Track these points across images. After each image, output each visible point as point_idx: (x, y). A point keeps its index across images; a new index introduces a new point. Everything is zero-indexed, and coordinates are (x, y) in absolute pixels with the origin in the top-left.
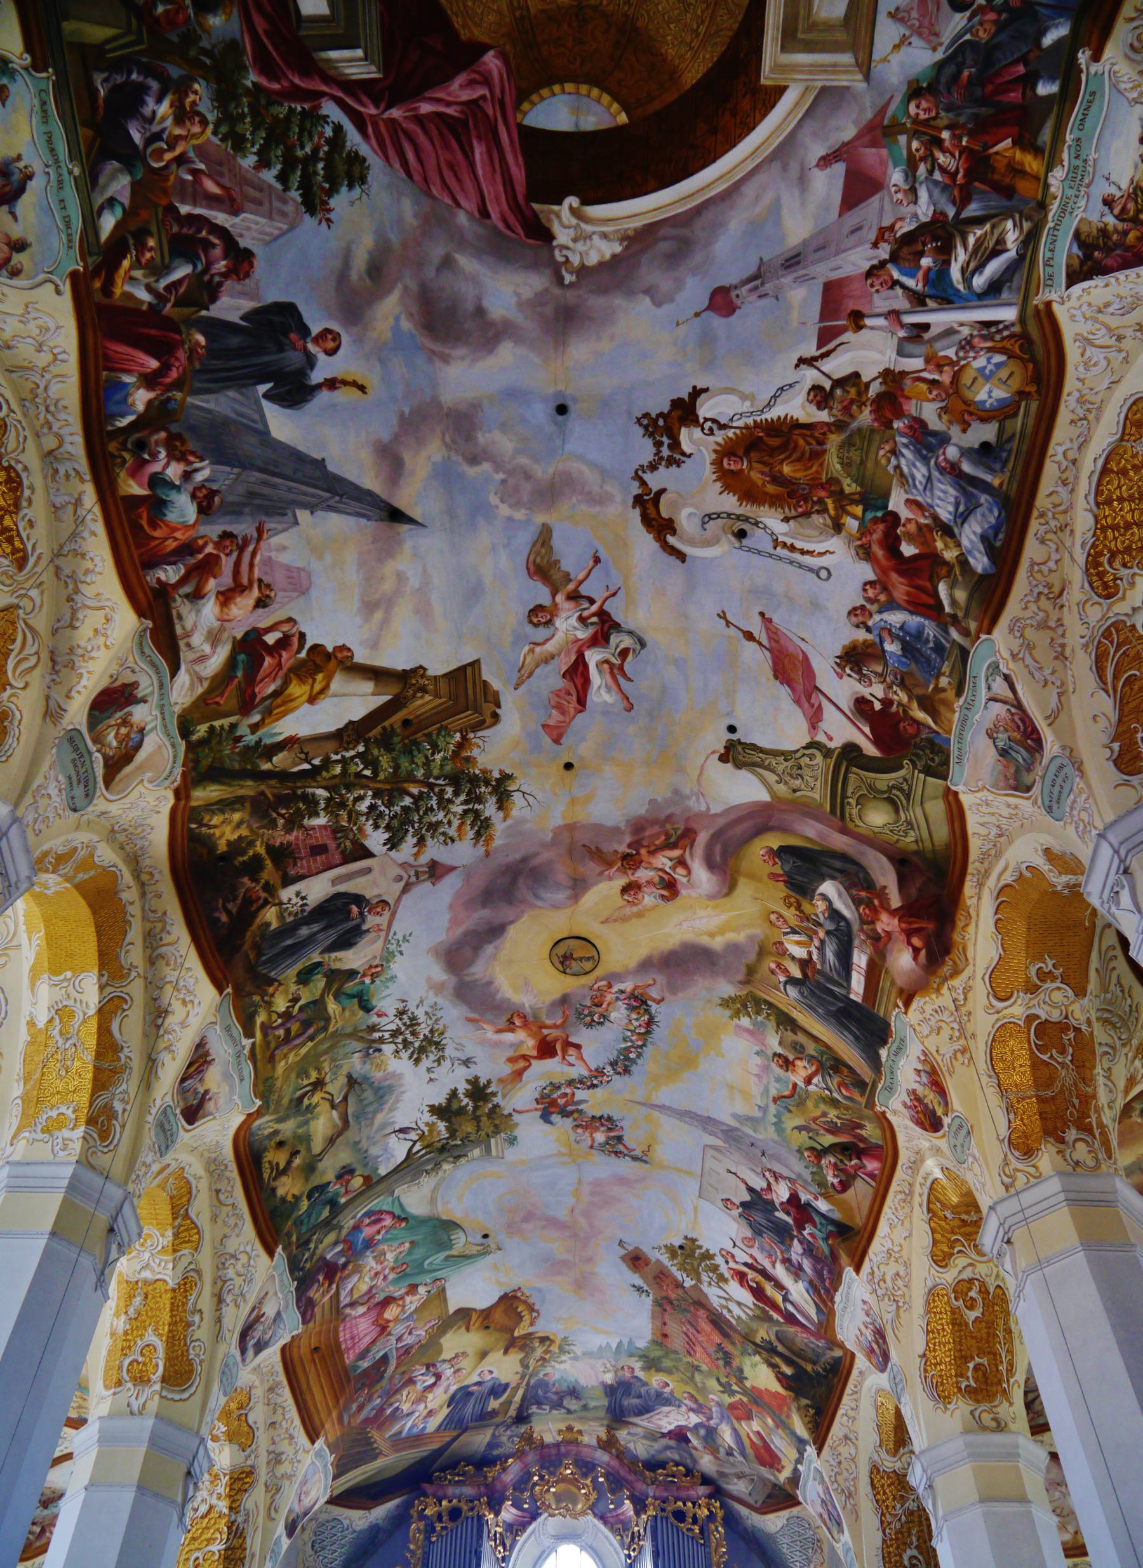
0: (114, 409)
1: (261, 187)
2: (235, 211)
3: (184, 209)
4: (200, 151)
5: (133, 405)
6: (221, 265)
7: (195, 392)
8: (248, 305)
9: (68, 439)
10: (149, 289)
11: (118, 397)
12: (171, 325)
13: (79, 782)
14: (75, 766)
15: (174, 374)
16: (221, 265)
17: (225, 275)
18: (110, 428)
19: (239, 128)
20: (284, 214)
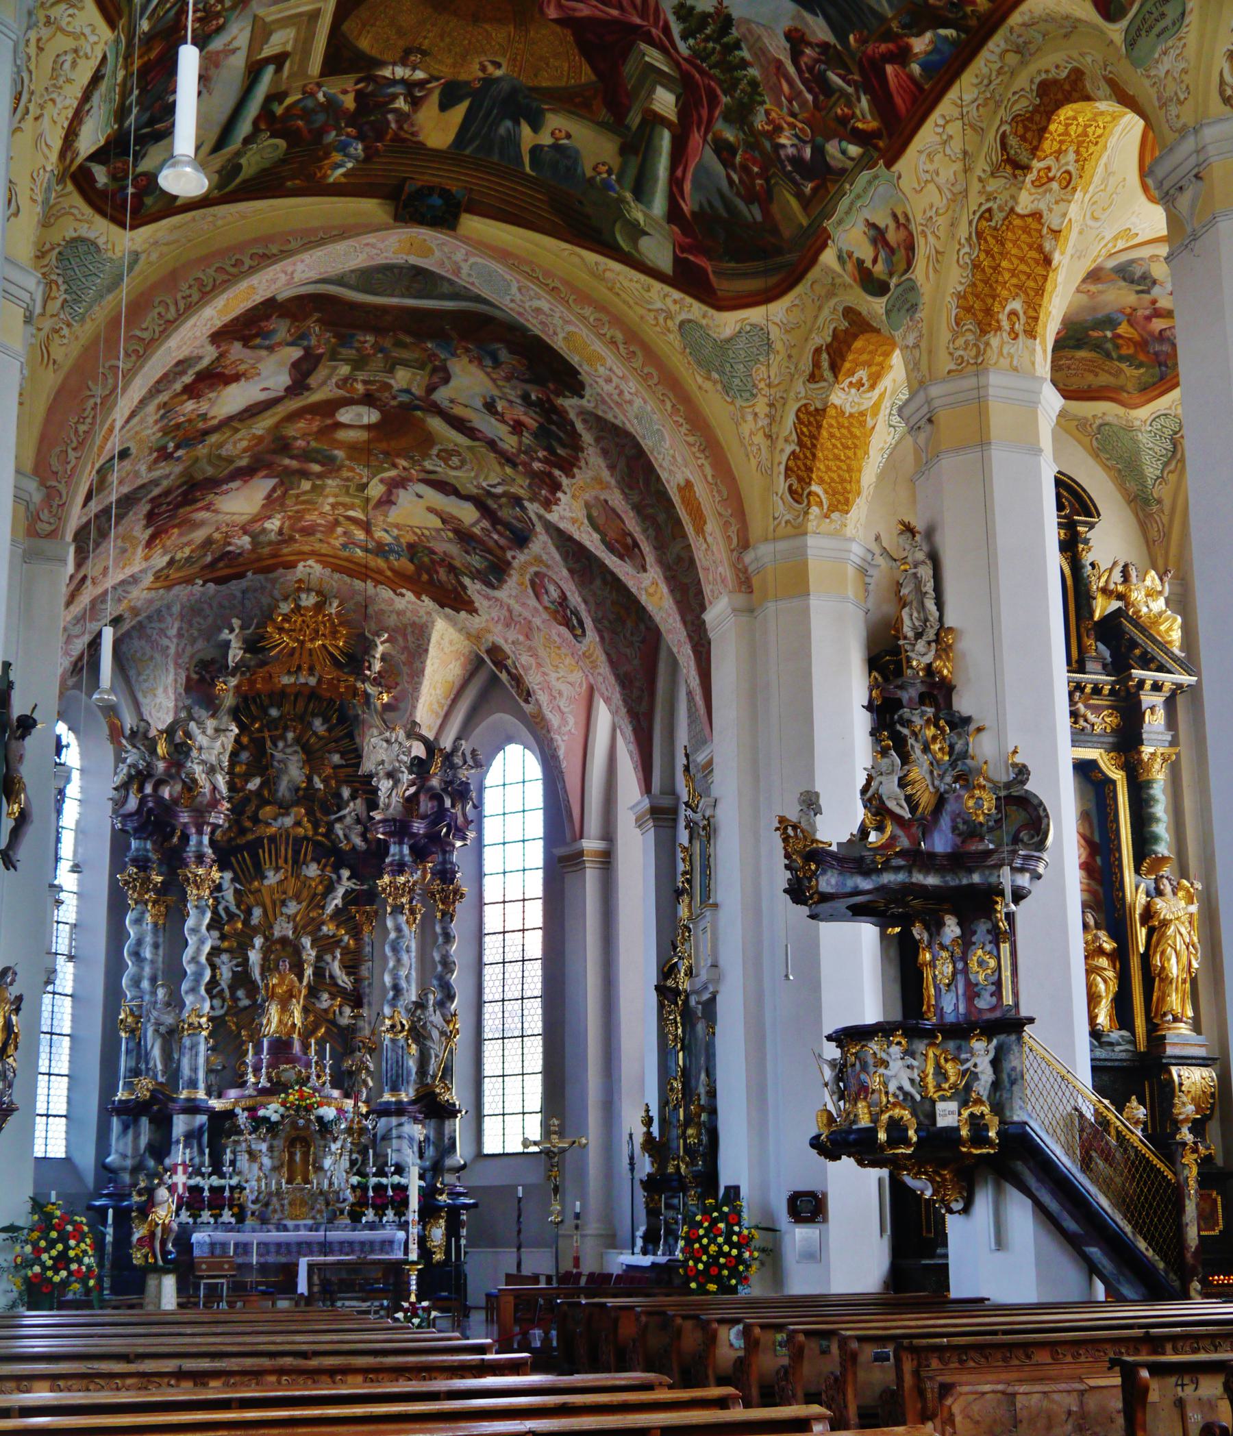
0: (946, 49)
1: (755, 55)
2: (779, 64)
3: (809, 97)
4: (780, 106)
5: (931, 42)
6: (808, 51)
7: (882, 19)
8: (808, 17)
9: (998, 51)
10: (859, 100)
11: (935, 57)
12: (862, 72)
13: (1163, 15)
14: (1151, 27)
15: (883, 48)
16: (808, 51)
17: (809, 44)
18: (963, 36)
19: (749, 89)
20: (750, 31)
